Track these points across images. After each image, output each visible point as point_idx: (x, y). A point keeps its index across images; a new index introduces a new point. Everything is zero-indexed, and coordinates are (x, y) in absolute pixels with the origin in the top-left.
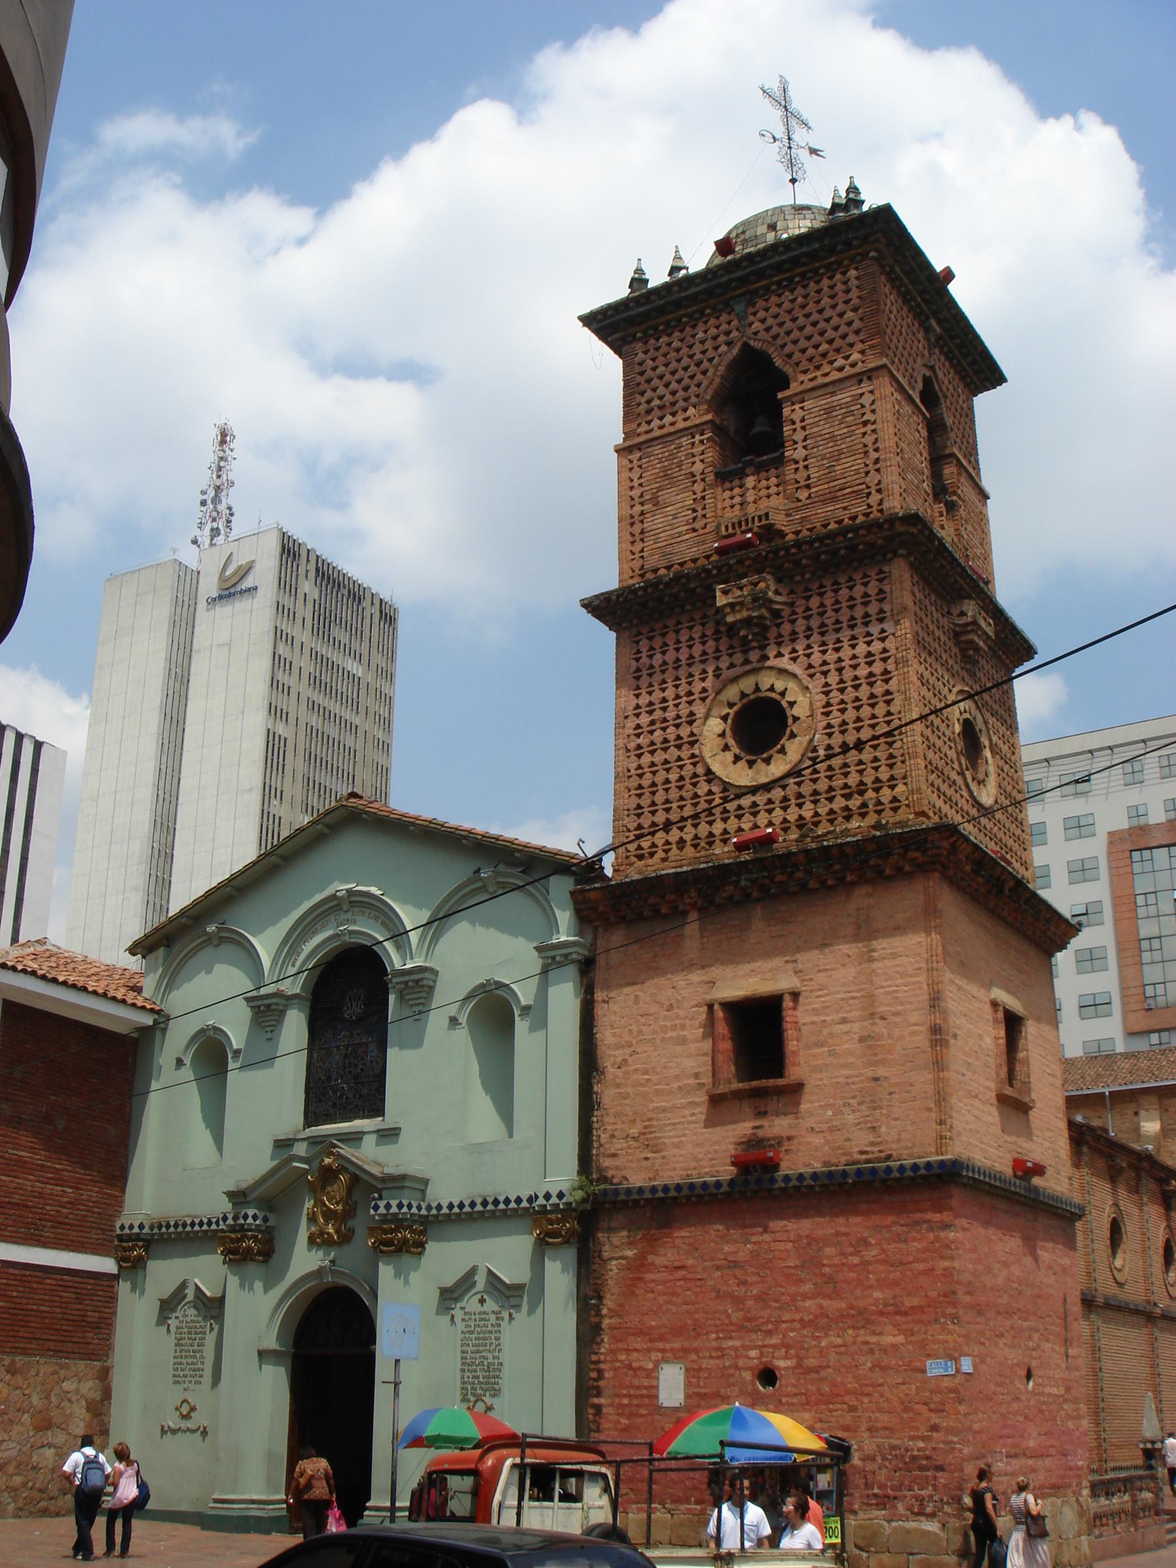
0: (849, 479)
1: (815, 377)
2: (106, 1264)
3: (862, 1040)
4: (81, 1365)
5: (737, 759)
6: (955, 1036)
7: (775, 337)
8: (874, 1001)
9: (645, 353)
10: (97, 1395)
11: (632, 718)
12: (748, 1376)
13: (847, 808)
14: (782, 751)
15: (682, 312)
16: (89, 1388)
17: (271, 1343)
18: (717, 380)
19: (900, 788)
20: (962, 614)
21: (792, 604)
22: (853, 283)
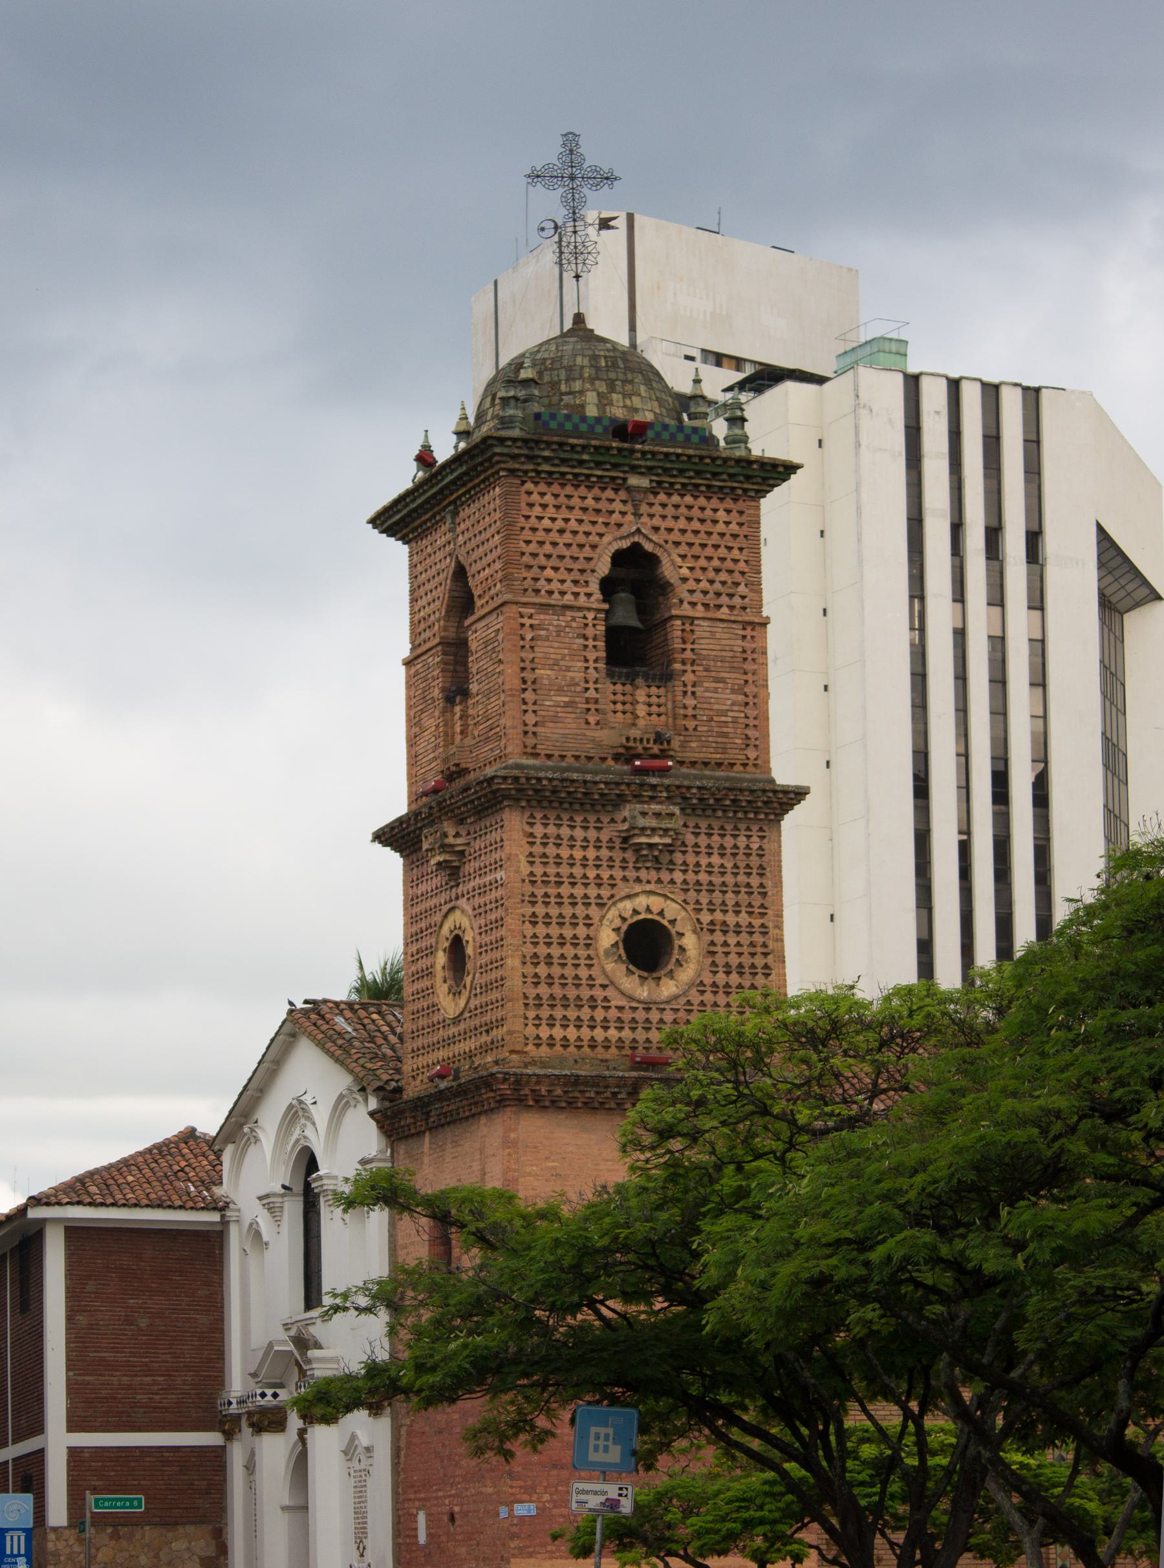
2: (211, 1438)
4: (190, 1529)
10: (211, 1551)
12: (446, 1518)
14: (465, 987)
16: (203, 1546)
17: (287, 1502)
21: (468, 844)
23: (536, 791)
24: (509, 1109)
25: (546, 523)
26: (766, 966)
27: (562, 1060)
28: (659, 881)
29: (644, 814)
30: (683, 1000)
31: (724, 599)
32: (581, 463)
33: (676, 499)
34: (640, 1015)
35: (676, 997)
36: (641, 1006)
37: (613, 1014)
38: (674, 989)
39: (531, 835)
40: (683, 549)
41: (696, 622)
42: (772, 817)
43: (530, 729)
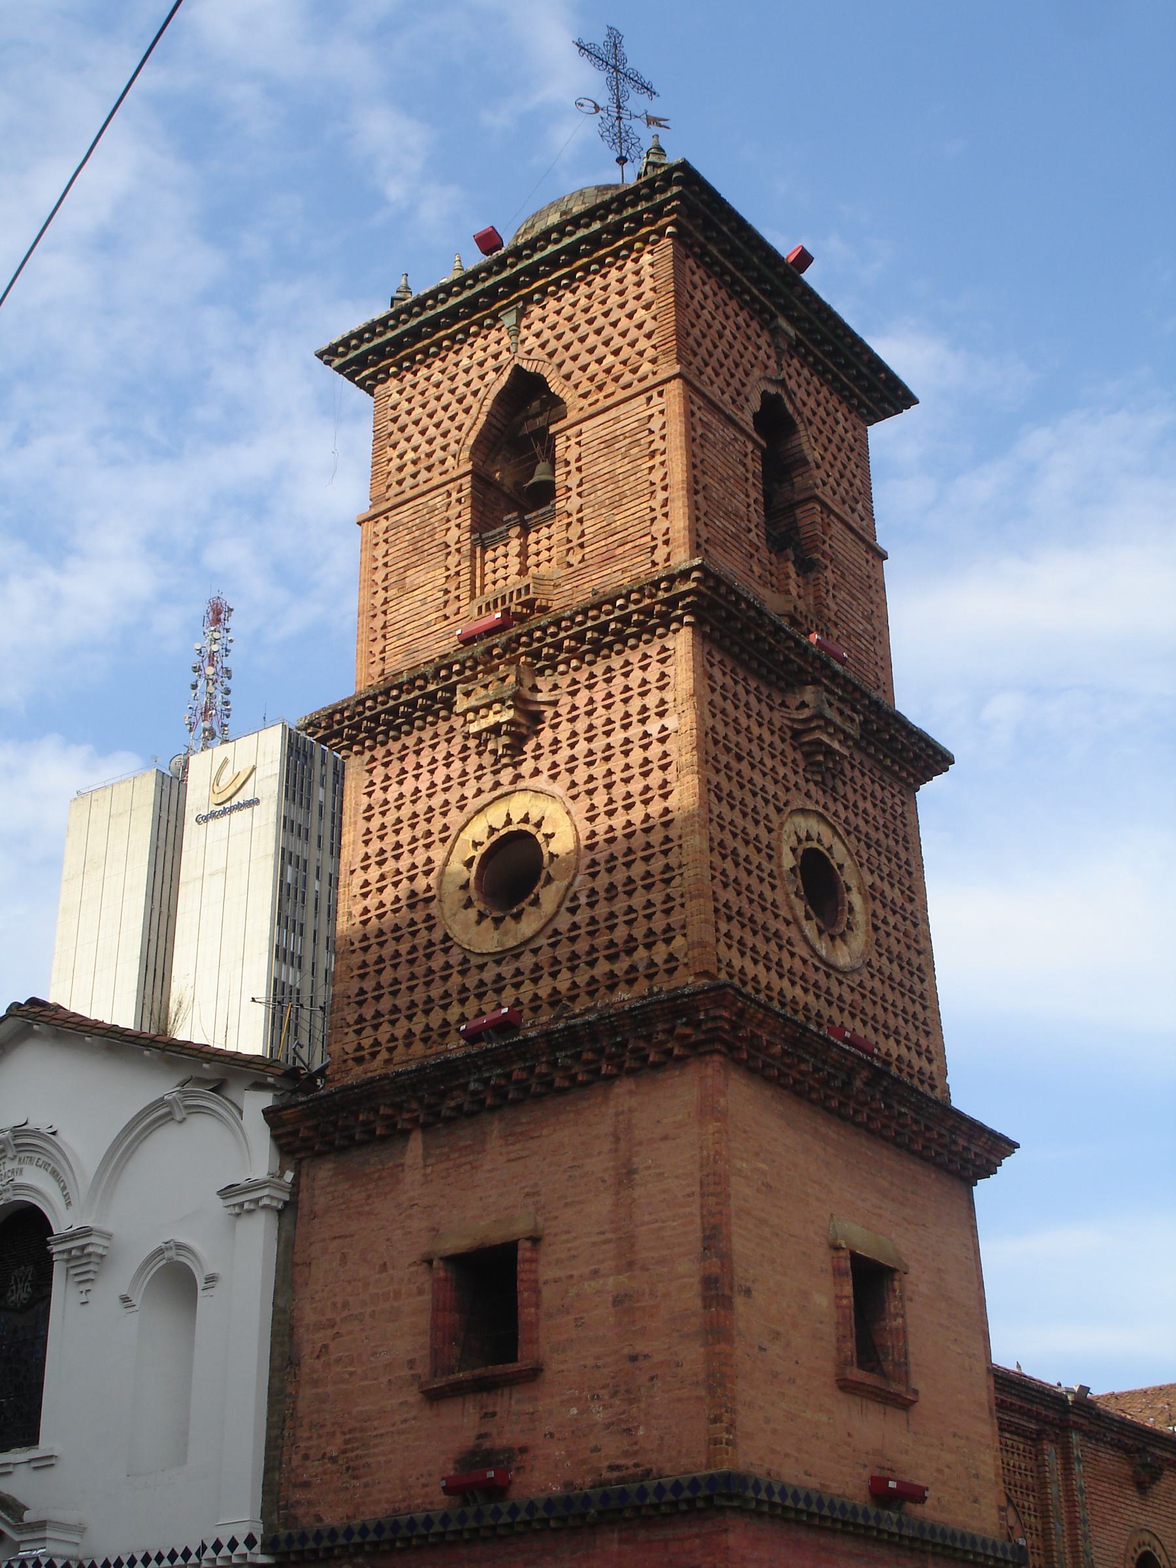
0: (631, 530)
1: (597, 401)
3: (617, 1301)
5: (482, 916)
6: (748, 1292)
7: (551, 355)
8: (633, 1246)
9: (400, 392)
11: (359, 872)
13: (612, 975)
14: (536, 902)
15: (442, 333)
18: (483, 418)
19: (679, 942)
20: (803, 705)
22: (647, 271)
23: (730, 617)
24: (717, 1058)
28: (825, 807)
29: (830, 705)
30: (857, 979)
35: (854, 970)
36: (823, 967)
38: (848, 959)
39: (711, 677)
41: (832, 517)
42: (912, 780)
43: (701, 541)
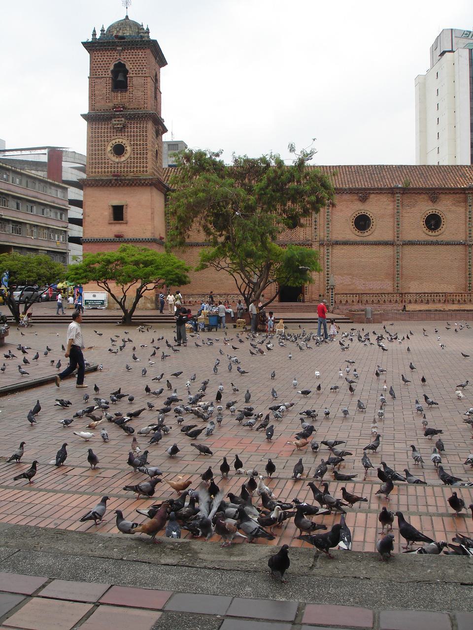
6: (89, 216)
25: (99, 60)
26: (147, 153)
27: (97, 176)
29: (115, 121)
30: (126, 161)
31: (140, 72)
32: (105, 46)
33: (129, 51)
34: (116, 165)
37: (110, 165)
40: (131, 62)
43: (93, 104)
